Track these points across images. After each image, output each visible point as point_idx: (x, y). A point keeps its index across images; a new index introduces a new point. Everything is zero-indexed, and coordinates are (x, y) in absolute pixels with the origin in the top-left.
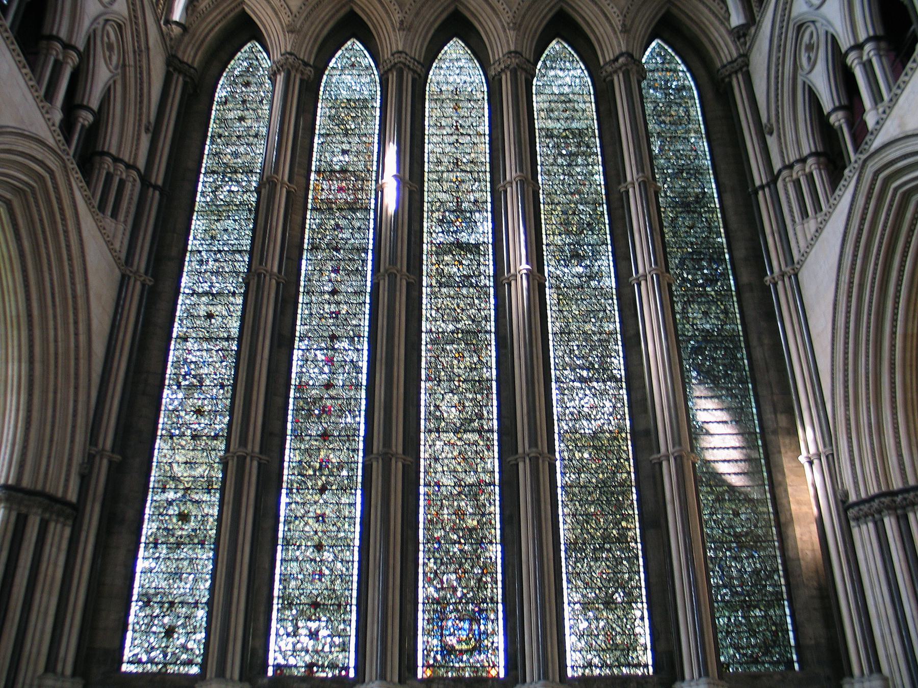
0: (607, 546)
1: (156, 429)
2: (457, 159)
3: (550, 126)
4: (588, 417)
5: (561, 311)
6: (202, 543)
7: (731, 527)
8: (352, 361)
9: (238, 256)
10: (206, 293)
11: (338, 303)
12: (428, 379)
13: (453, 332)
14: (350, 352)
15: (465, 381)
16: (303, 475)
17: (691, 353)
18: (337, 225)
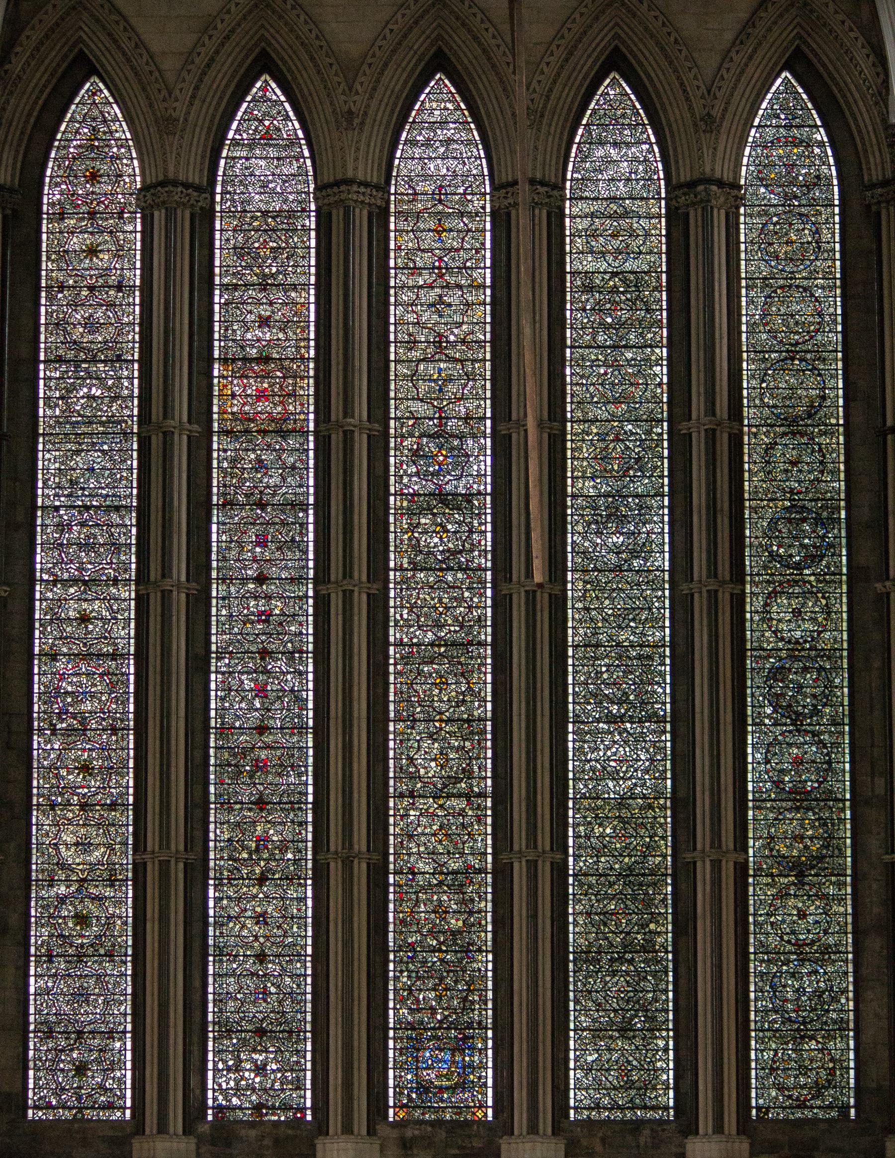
0: (628, 956)
1: (30, 796)
2: (440, 335)
3: (589, 268)
4: (614, 776)
5: (587, 609)
6: (110, 955)
7: (793, 932)
8: (292, 691)
9: (115, 518)
10: (74, 581)
11: (268, 598)
12: (398, 719)
13: (432, 644)
14: (289, 677)
15: (449, 721)
16: (235, 860)
17: (768, 678)
18: (259, 461)
